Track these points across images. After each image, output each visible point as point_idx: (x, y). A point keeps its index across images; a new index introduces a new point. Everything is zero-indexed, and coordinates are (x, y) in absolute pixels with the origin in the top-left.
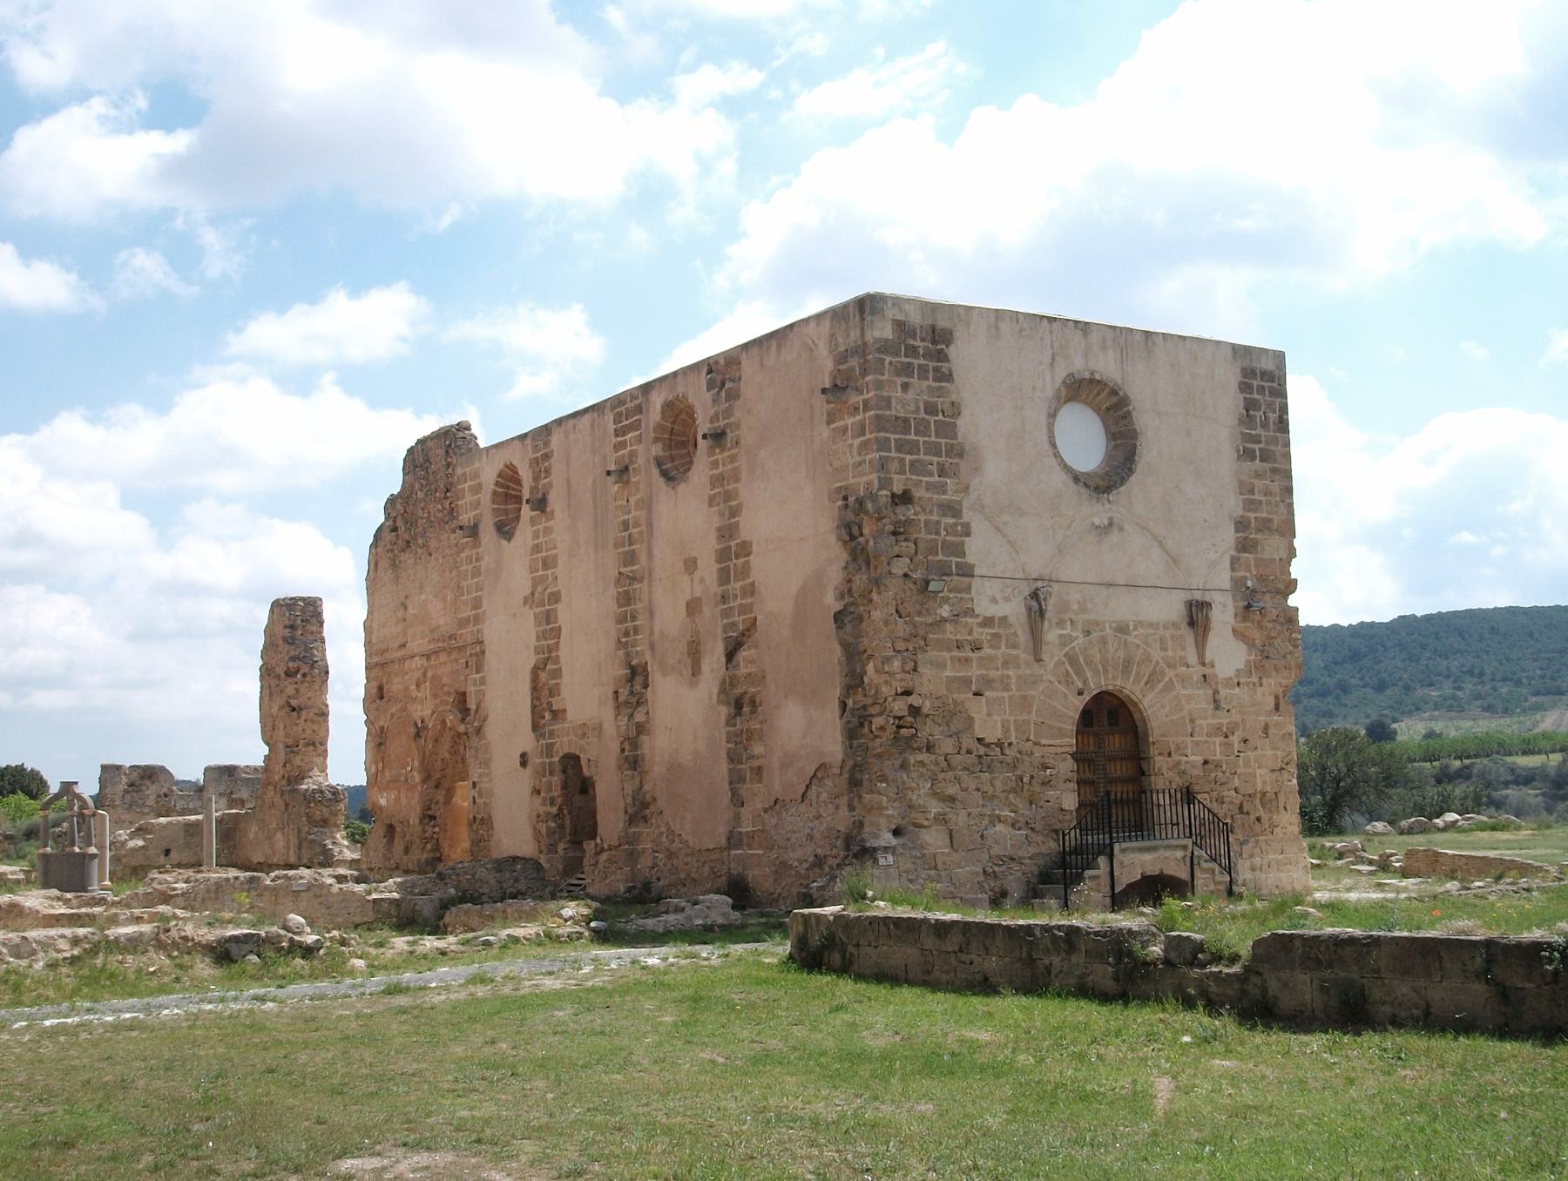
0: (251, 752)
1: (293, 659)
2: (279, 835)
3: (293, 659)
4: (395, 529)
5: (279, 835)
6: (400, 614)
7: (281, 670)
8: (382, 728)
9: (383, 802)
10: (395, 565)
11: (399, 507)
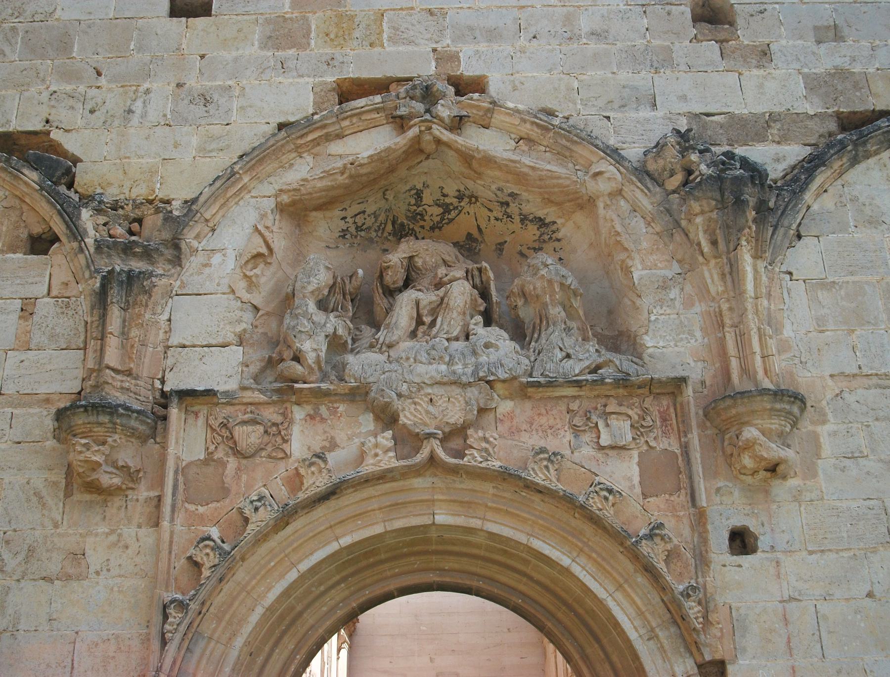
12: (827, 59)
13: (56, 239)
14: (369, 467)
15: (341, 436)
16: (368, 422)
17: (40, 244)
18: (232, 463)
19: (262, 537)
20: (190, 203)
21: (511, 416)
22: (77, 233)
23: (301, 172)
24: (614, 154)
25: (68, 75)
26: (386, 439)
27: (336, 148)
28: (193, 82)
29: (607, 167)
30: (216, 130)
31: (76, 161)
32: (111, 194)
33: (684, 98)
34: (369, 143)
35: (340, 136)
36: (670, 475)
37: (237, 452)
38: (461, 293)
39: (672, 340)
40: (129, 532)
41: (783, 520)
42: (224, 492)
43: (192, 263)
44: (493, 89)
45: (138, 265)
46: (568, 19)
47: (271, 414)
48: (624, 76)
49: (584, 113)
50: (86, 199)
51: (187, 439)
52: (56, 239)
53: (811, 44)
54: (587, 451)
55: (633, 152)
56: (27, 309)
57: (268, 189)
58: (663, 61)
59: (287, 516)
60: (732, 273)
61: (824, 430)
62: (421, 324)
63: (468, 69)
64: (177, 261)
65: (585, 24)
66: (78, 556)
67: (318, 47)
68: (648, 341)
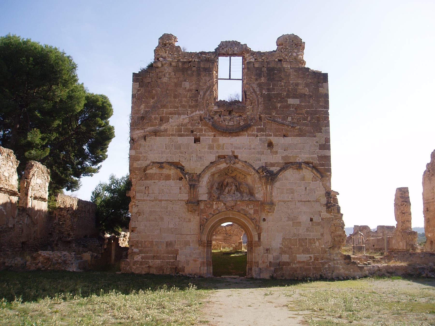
0: (393, 223)
1: (403, 201)
2: (401, 242)
3: (403, 201)
4: (429, 171)
5: (401, 242)
6: (432, 191)
7: (399, 204)
8: (428, 218)
9: (429, 235)
10: (430, 180)
11: (430, 166)
12: (285, 154)
13: (182, 178)
14: (223, 210)
15: (219, 206)
16: (222, 204)
17: (181, 179)
18: (207, 209)
19: (211, 218)
20: (200, 174)
21: (239, 204)
22: (186, 178)
23: (213, 170)
24: (254, 169)
25: (181, 153)
26: (224, 207)
27: (218, 166)
28: (198, 155)
29: (253, 171)
30: (202, 163)
31: (184, 167)
32: (189, 172)
33: (264, 160)
34: (223, 166)
35: (219, 164)
36: (256, 212)
37: (207, 207)
38: (234, 188)
39: (259, 196)
40: (195, 217)
41: (270, 218)
42: (206, 212)
43: (201, 183)
44: (239, 158)
45: (194, 183)
46: (250, 146)
47: (211, 203)
48: (257, 155)
49: (251, 162)
50: (187, 173)
51: (202, 206)
52: (182, 178)
53: (283, 151)
54: (248, 209)
55: (257, 168)
56: (180, 189)
57: (210, 172)
58: (262, 153)
59: (213, 215)
60: (266, 188)
61: (275, 207)
62: (229, 192)
63: (236, 154)
64: (199, 182)
65: (252, 147)
66: (190, 219)
67: (215, 150)
68: (256, 195)
